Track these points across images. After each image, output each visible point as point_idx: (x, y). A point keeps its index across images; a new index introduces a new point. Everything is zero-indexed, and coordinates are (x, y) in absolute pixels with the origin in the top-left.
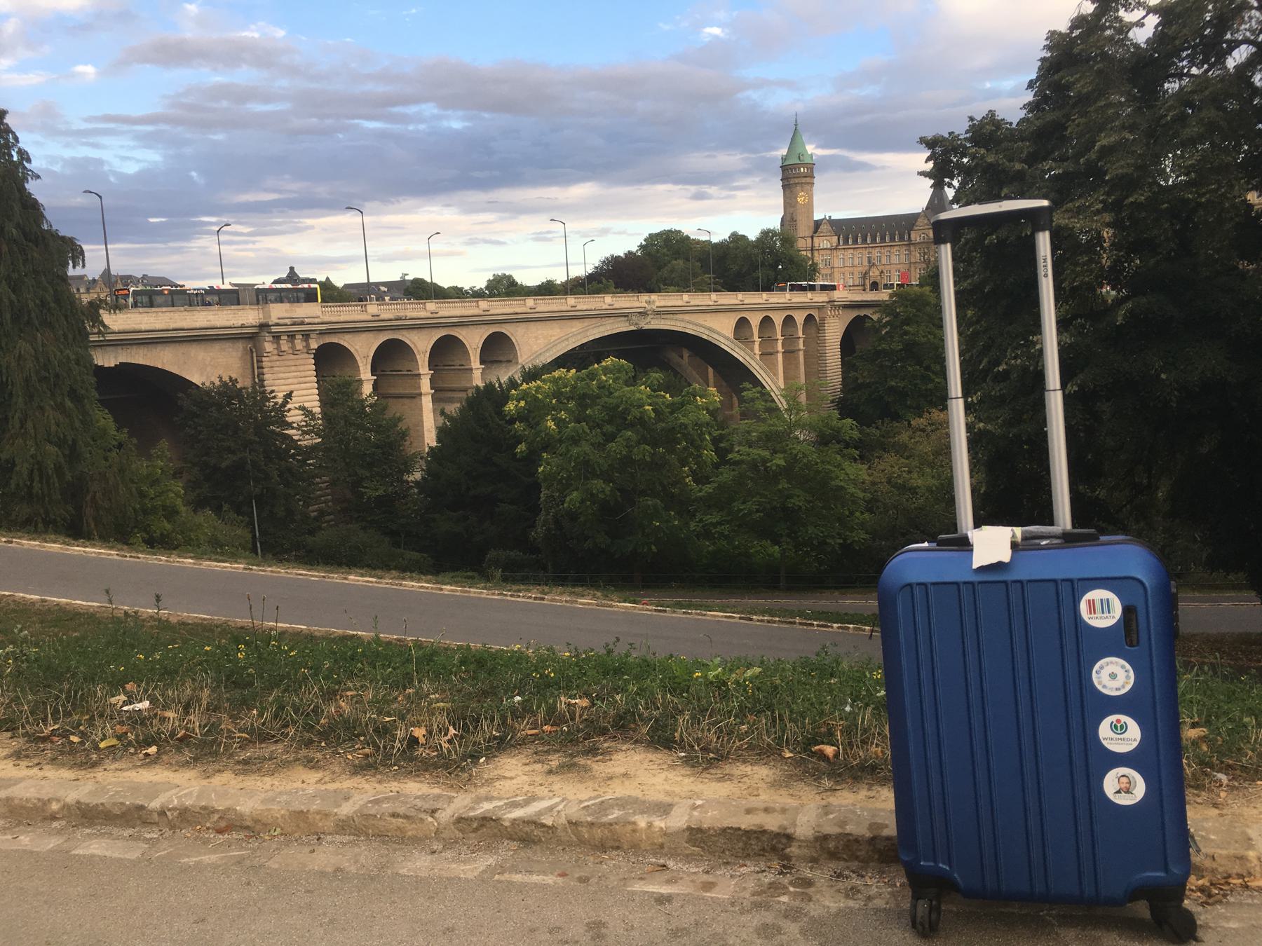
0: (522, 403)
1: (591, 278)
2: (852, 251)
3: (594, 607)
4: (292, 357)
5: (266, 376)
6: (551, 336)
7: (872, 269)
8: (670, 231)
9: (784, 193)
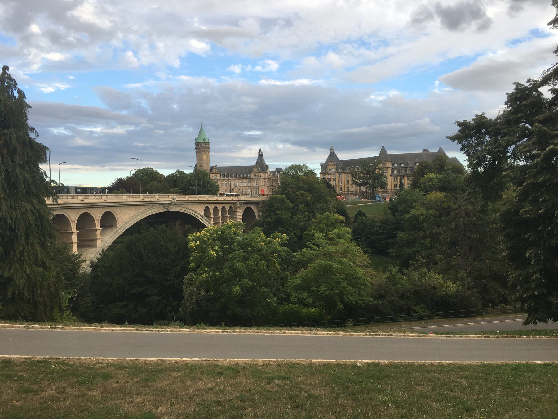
0: (198, 243)
1: (109, 188)
2: (226, 180)
3: (417, 337)
6: (131, 214)
7: (235, 188)
8: (148, 168)
9: (197, 154)
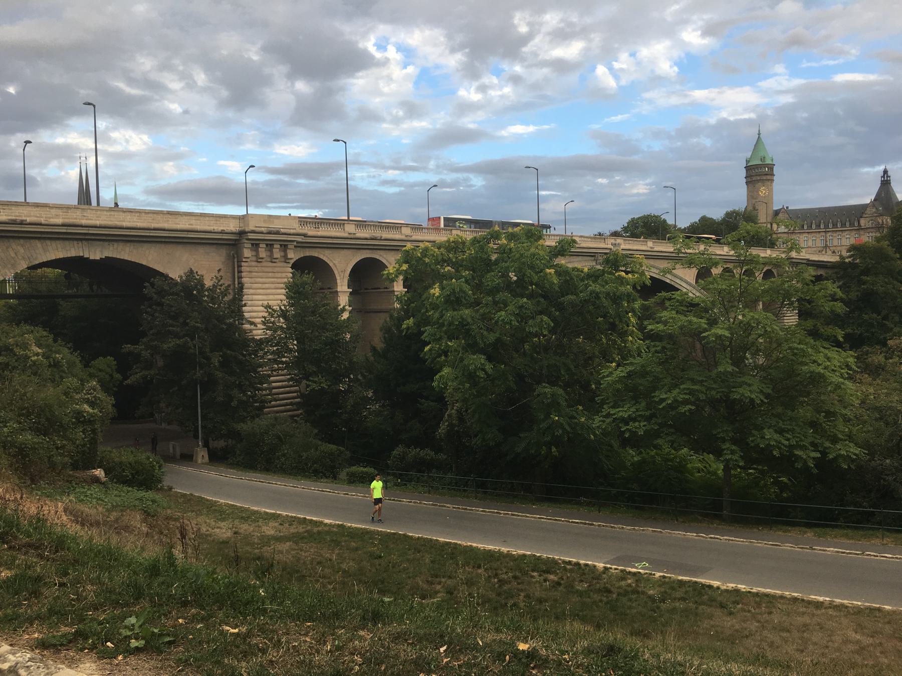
4: (271, 264)
5: (244, 280)
9: (748, 188)
